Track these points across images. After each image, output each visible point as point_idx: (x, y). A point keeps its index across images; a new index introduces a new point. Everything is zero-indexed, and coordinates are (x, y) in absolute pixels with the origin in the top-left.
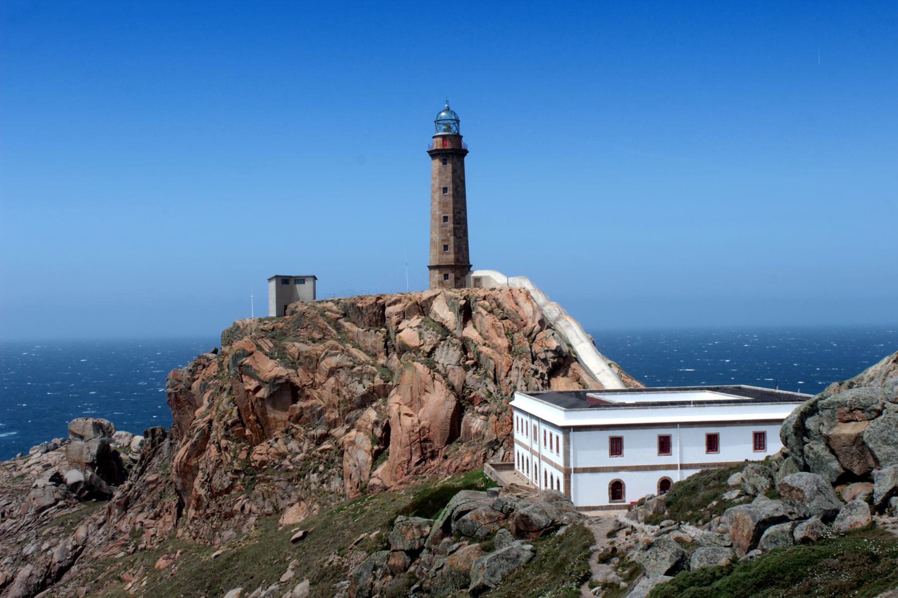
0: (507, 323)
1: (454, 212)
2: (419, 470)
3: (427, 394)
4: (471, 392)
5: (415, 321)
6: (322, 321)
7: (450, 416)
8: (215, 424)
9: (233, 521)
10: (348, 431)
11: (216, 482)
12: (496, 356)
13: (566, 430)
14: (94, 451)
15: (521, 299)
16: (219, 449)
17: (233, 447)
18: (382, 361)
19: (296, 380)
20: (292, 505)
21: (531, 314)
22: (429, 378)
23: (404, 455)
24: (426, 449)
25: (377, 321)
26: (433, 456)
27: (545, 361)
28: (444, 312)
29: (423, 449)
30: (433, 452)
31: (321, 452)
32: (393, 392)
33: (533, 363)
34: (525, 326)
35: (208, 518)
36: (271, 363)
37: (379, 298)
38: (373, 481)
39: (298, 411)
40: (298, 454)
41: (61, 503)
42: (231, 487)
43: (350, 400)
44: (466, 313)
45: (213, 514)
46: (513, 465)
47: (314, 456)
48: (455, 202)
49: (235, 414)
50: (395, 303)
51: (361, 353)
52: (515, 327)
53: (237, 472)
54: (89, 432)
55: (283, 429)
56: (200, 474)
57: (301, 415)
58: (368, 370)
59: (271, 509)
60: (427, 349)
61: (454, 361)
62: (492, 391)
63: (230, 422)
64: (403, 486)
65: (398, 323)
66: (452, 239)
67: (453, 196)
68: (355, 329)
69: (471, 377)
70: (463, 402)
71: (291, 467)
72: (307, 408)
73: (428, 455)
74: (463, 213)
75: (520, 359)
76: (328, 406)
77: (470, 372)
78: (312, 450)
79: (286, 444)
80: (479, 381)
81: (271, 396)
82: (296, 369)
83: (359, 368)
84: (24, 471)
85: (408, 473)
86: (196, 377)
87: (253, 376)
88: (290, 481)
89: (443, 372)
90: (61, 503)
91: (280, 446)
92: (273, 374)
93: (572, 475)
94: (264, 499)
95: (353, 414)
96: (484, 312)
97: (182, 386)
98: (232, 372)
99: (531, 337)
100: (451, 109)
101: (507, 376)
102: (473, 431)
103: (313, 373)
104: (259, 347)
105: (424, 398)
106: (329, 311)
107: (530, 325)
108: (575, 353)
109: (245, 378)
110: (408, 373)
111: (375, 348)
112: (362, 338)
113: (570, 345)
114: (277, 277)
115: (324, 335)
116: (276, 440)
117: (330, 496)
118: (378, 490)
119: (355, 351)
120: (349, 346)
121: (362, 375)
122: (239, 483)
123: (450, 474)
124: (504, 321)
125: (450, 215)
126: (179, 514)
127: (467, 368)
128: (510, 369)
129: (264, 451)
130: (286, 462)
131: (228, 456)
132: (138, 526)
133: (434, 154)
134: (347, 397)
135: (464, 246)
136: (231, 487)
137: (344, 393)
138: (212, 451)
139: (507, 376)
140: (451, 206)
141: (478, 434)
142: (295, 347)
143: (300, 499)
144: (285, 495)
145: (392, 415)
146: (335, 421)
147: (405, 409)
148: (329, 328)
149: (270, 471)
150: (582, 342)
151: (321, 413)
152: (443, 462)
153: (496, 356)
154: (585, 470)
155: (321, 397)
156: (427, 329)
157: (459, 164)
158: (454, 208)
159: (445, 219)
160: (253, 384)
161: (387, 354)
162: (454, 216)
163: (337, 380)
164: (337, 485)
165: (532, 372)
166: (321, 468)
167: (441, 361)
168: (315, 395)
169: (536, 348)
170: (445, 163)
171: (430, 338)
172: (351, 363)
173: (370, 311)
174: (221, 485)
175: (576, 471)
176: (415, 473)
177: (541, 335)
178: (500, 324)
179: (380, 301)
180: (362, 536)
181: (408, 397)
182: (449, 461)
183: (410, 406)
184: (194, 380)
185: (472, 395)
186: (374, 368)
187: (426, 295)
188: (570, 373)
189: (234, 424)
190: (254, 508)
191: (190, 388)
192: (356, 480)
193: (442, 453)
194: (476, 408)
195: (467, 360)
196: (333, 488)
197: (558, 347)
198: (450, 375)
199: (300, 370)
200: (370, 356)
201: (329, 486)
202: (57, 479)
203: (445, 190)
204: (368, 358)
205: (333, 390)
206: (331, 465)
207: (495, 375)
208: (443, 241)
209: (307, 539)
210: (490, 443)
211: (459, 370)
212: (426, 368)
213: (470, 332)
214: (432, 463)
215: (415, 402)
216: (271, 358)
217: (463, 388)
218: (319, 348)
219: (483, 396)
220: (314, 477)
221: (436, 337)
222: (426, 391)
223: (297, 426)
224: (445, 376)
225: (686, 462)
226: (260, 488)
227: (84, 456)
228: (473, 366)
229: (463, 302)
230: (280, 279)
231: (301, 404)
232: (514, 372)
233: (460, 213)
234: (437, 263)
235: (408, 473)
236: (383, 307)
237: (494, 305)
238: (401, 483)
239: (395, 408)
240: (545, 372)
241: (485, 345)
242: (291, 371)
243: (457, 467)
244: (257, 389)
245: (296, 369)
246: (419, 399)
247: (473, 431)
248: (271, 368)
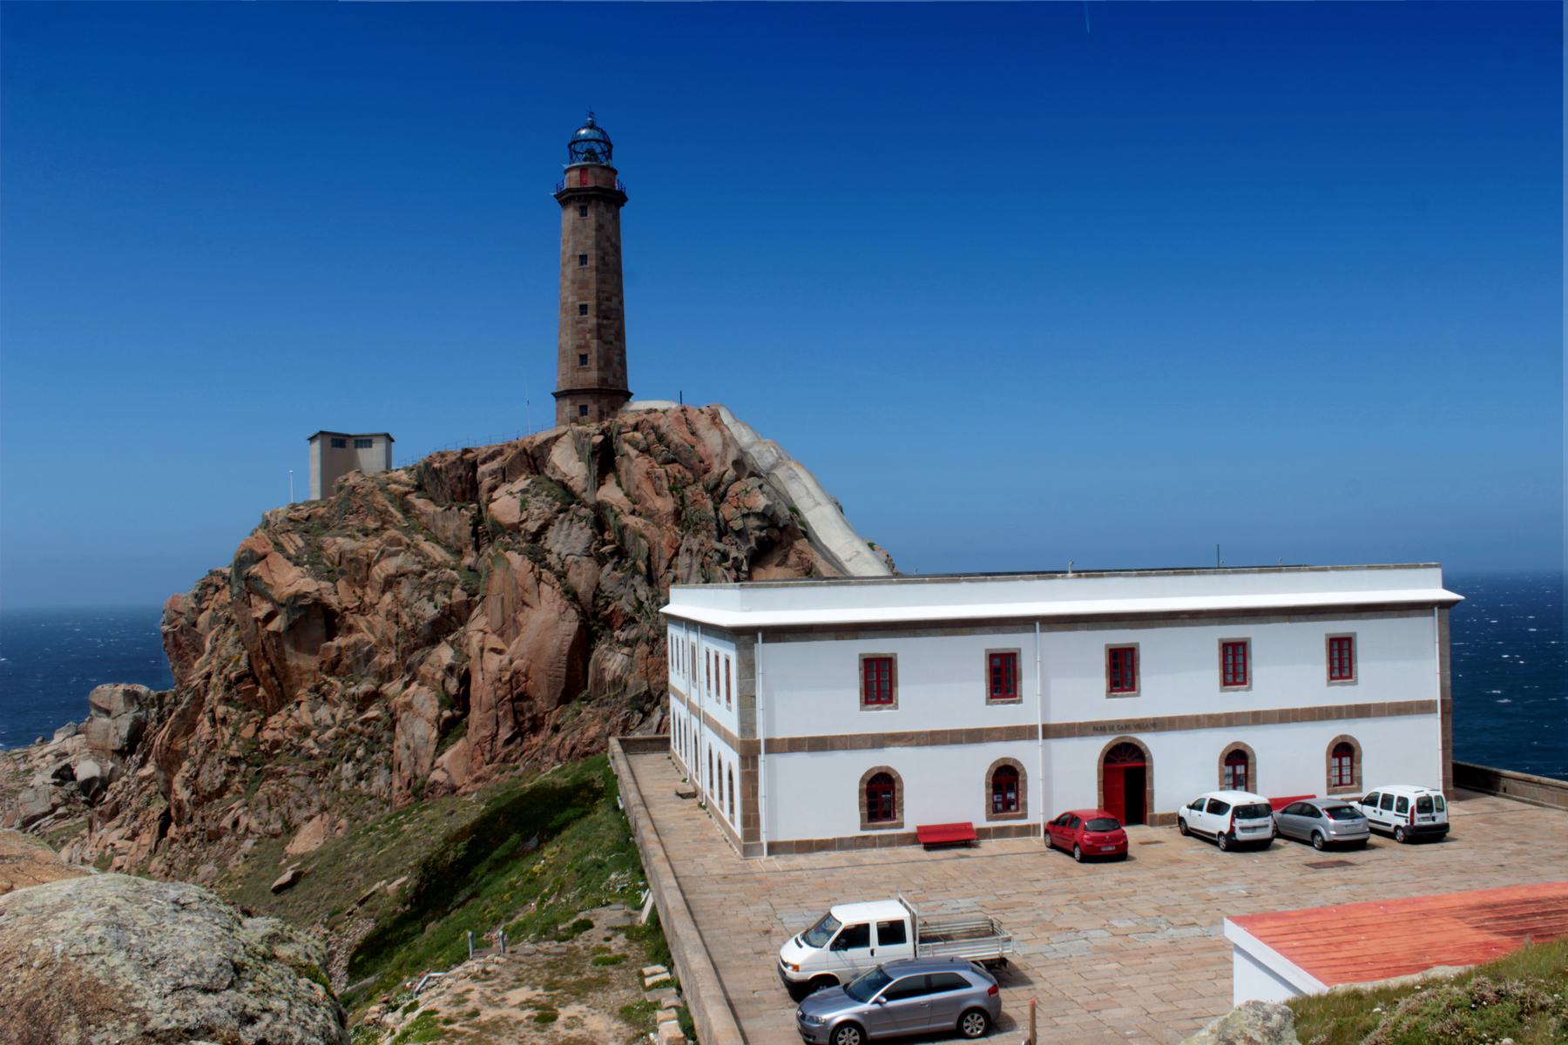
0: (674, 469)
1: (598, 298)
2: (509, 754)
3: (527, 609)
4: (608, 604)
5: (522, 483)
6: (381, 500)
7: (566, 649)
8: (214, 679)
9: (216, 849)
10: (407, 685)
11: (204, 778)
12: (652, 531)
13: (743, 636)
14: (124, 732)
15: (702, 424)
16: (213, 721)
17: (235, 717)
18: (468, 561)
19: (333, 600)
20: (309, 819)
21: (719, 449)
22: (531, 579)
23: (484, 726)
24: (522, 713)
25: (464, 492)
26: (536, 728)
27: (740, 533)
28: (568, 463)
29: (517, 713)
30: (534, 719)
31: (362, 723)
32: (476, 611)
33: (720, 540)
34: (706, 471)
35: (187, 841)
36: (297, 571)
37: (466, 451)
38: (437, 775)
39: (333, 654)
40: (328, 727)
41: (60, 810)
42: (225, 787)
43: (413, 630)
44: (604, 460)
45: (194, 834)
46: (668, 740)
47: (352, 731)
48: (601, 281)
49: (243, 663)
50: (492, 457)
51: (438, 548)
52: (689, 475)
53: (235, 761)
54: (118, 704)
55: (311, 685)
56: (186, 765)
57: (338, 660)
58: (445, 577)
59: (277, 826)
60: (532, 526)
61: (580, 548)
62: (643, 599)
63: (233, 675)
64: (480, 785)
65: (493, 489)
66: (594, 343)
67: (597, 269)
68: (431, 508)
69: (609, 576)
70: (594, 622)
71: (316, 751)
72: (348, 648)
73: (527, 725)
74: (615, 300)
75: (696, 533)
76: (381, 642)
77: (608, 567)
78: (348, 721)
79: (312, 711)
80: (622, 583)
81: (291, 628)
82: (334, 581)
83: (431, 574)
84: (35, 763)
85: (492, 760)
86: (204, 605)
87: (265, 596)
88: (312, 775)
89: (558, 568)
90: (60, 810)
91: (303, 715)
92: (292, 590)
93: (762, 757)
94: (270, 809)
95: (417, 655)
96: (633, 452)
97: (183, 621)
98: (236, 590)
99: (718, 493)
100: (598, 125)
101: (669, 567)
102: (608, 677)
103: (363, 587)
104: (279, 547)
105: (521, 618)
106: (395, 482)
107: (716, 469)
108: (803, 524)
109: (254, 600)
110: (498, 574)
111: (458, 538)
112: (440, 524)
113: (794, 510)
114: (322, 433)
115: (384, 523)
116: (298, 704)
117: (369, 803)
118: (440, 791)
119: (427, 547)
120: (420, 538)
121: (435, 585)
122: (237, 779)
123: (559, 759)
124: (668, 467)
125: (591, 303)
126: (163, 832)
127: (601, 560)
128: (676, 554)
129: (279, 725)
130: (309, 743)
131: (227, 732)
132: (109, 851)
133: (566, 198)
134: (409, 625)
135: (617, 359)
136: (225, 787)
137: (405, 618)
138: (204, 729)
139: (669, 567)
140: (593, 286)
141: (617, 682)
142: (338, 544)
143: (324, 809)
144: (303, 802)
145: (472, 654)
146: (390, 668)
147: (494, 641)
148: (392, 510)
149: (285, 757)
150: (818, 504)
151: (369, 656)
152: (550, 738)
153: (652, 531)
154: (795, 745)
155: (371, 629)
156: (537, 495)
157: (609, 216)
158: (598, 291)
159: (583, 309)
160: (263, 609)
161: (477, 548)
162: (599, 305)
163: (395, 597)
164: (382, 783)
165: (717, 557)
166: (360, 752)
167: (556, 549)
168: (363, 625)
169: (727, 511)
170: (583, 213)
171: (540, 508)
172: (420, 567)
173: (452, 474)
174: (211, 783)
175: (773, 746)
176: (504, 760)
177: (737, 487)
178: (660, 471)
179: (469, 456)
180: (377, 886)
181: (497, 617)
182: (561, 735)
183: (501, 635)
184: (201, 611)
185: (611, 608)
186: (455, 573)
187: (541, 437)
188: (793, 559)
189: (240, 679)
190: (254, 824)
191: (195, 625)
192: (407, 773)
193: (550, 721)
194: (617, 633)
195: (604, 543)
196: (374, 789)
197: (767, 507)
198: (570, 574)
199: (341, 584)
200: (452, 553)
201: (370, 785)
202: (65, 775)
203: (583, 259)
204: (448, 557)
205: (388, 613)
206: (376, 747)
207: (649, 567)
208: (579, 347)
209: (298, 888)
210: (636, 698)
211: (588, 565)
212: (527, 561)
213: (610, 493)
214: (534, 740)
215: (508, 628)
216: (296, 564)
217: (595, 596)
218: (373, 544)
219: (628, 609)
220: (348, 769)
221: (552, 505)
222: (525, 604)
223: (331, 679)
224: (561, 576)
225: (1055, 719)
226: (269, 787)
227: (111, 740)
228: (612, 554)
229: (598, 439)
230: (329, 439)
231: (339, 641)
232: (683, 560)
233: (609, 299)
234: (568, 387)
235: (492, 760)
236: (474, 466)
237: (652, 437)
238: (477, 780)
239: (476, 639)
240: (741, 556)
241: (633, 513)
242: (324, 584)
243: (573, 748)
244: (270, 617)
245: (334, 581)
246: (514, 620)
247: (608, 677)
248: (290, 579)
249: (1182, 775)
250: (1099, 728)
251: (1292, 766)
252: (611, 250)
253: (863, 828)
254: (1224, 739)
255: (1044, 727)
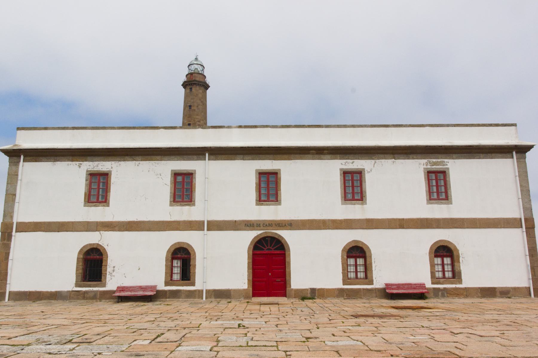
100: (199, 59)
175: (24, 227)
249: (313, 262)
250: (249, 225)
251: (401, 260)
252: (201, 104)
253: (77, 285)
254: (348, 237)
255: (208, 222)
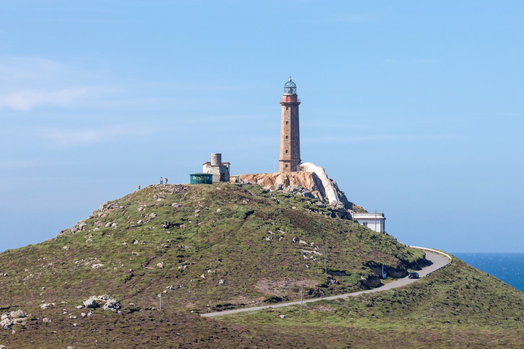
48: (292, 129)
66: (290, 147)
74: (296, 134)
125: (289, 135)
157: (295, 109)
159: (287, 137)
162: (291, 136)
179: (255, 177)
203: (287, 123)
